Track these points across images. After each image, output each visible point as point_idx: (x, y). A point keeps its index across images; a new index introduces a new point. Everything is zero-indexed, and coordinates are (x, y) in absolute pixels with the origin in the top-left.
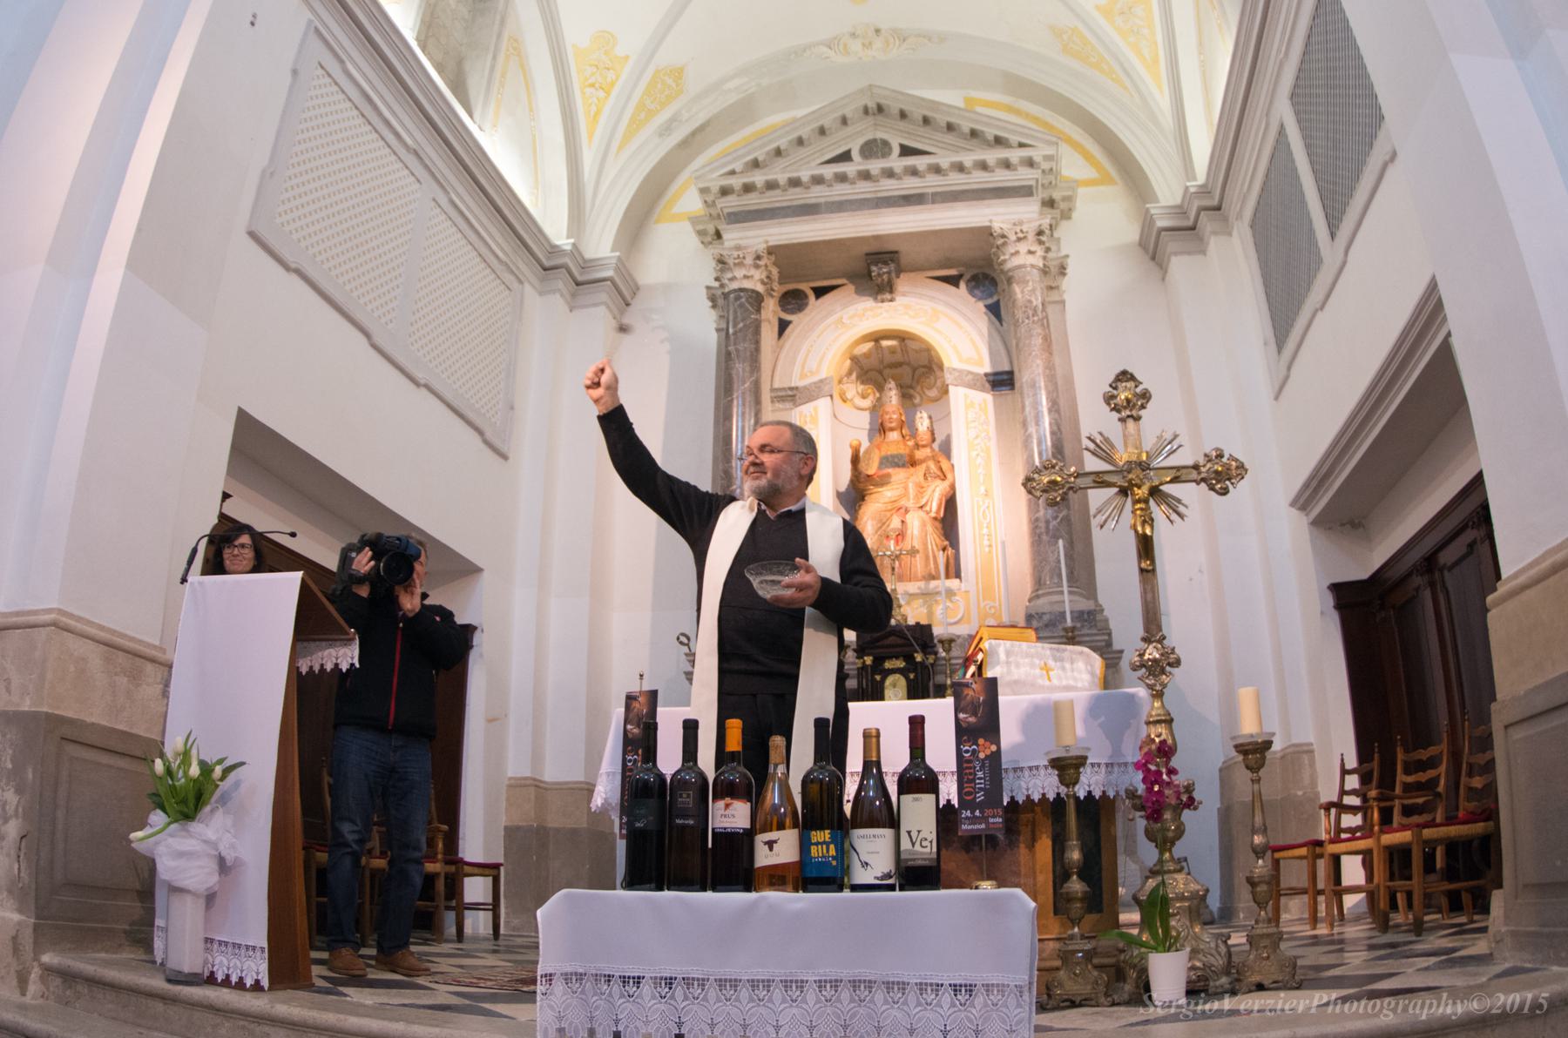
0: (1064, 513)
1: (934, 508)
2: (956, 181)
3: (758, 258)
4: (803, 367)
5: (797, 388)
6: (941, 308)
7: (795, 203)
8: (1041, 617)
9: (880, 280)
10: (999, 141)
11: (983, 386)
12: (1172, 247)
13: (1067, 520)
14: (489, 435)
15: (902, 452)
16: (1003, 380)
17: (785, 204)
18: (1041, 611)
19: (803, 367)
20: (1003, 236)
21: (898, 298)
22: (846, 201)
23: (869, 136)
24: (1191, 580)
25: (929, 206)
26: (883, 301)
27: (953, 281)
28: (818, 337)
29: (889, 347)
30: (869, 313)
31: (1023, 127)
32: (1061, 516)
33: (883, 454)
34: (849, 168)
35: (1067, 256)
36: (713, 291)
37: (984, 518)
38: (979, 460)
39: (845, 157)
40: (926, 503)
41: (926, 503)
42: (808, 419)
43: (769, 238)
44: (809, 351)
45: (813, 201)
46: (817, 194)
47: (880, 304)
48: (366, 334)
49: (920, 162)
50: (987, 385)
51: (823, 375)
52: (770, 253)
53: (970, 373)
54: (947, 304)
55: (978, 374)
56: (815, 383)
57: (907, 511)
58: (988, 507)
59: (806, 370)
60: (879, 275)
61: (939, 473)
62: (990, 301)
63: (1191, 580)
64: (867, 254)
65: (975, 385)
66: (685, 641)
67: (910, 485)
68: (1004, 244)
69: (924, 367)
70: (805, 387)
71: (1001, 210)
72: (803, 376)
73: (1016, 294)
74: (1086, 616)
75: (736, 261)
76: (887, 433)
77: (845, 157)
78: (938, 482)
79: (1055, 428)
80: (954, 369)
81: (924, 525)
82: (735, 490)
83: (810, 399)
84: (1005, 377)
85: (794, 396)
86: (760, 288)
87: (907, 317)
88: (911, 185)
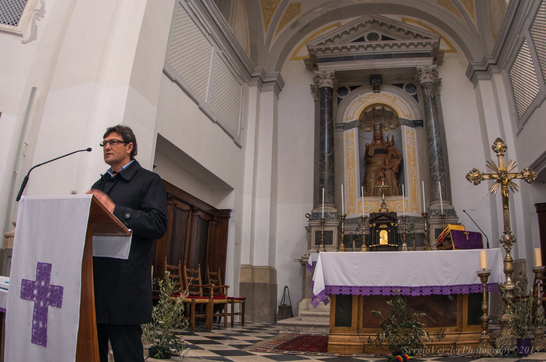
0: (443, 173)
1: (395, 170)
2: (404, 49)
3: (332, 75)
5: (345, 124)
6: (396, 96)
7: (344, 56)
9: (375, 85)
10: (417, 35)
11: (412, 125)
12: (479, 77)
13: (444, 176)
14: (236, 139)
15: (382, 148)
16: (419, 123)
17: (341, 56)
18: (435, 209)
19: (347, 116)
20: (420, 71)
21: (381, 92)
22: (363, 55)
23: (370, 32)
25: (394, 59)
26: (375, 92)
27: (400, 86)
28: (352, 105)
29: (378, 109)
30: (370, 97)
31: (427, 31)
32: (442, 174)
33: (375, 148)
34: (365, 44)
35: (441, 79)
36: (313, 87)
37: (413, 173)
38: (411, 153)
39: (362, 39)
40: (392, 167)
41: (392, 168)
42: (349, 135)
43: (335, 68)
44: (349, 111)
45: (351, 55)
46: (353, 53)
47: (375, 94)
48: (197, 103)
49: (390, 43)
50: (414, 125)
51: (355, 120)
52: (335, 74)
53: (408, 120)
54: (399, 95)
55: (411, 121)
56: (352, 122)
57: (385, 170)
58: (414, 170)
60: (375, 83)
61: (396, 156)
64: (370, 76)
65: (409, 125)
66: (309, 216)
67: (387, 160)
68: (421, 74)
69: (389, 117)
70: (348, 123)
71: (419, 61)
72: (347, 119)
73: (425, 93)
74: (451, 211)
75: (324, 77)
76: (376, 141)
77: (362, 39)
78: (396, 160)
80: (402, 119)
81: (391, 175)
82: (325, 161)
83: (350, 128)
84: (420, 122)
85: (344, 126)
86: (332, 86)
88: (387, 50)
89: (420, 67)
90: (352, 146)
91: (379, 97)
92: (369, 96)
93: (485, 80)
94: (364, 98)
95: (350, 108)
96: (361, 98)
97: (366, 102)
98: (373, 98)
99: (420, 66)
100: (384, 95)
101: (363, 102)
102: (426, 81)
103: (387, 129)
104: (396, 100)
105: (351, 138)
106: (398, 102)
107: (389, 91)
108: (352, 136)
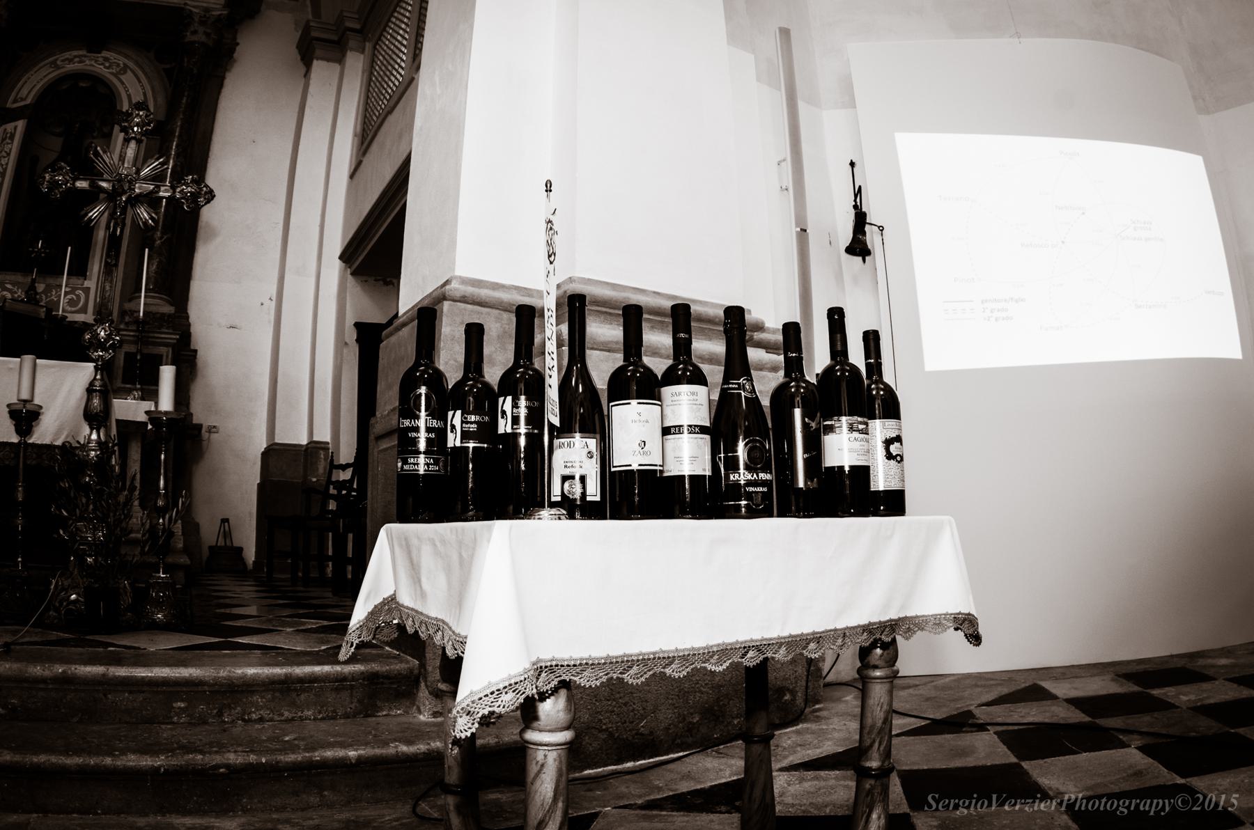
4: (17, 96)
8: (132, 314)
24: (262, 304)
28: (36, 72)
30: (77, 59)
32: (165, 237)
44: (26, 82)
59: (19, 96)
62: (168, 66)
63: (262, 304)
72: (15, 101)
74: (166, 318)
79: (179, 169)
87: (101, 67)
89: (190, 8)
90: (7, 159)
91: (93, 63)
92: (76, 57)
93: (328, 60)
94: (62, 61)
95: (29, 78)
96: (57, 60)
97: (63, 67)
98: (80, 62)
99: (194, 7)
100: (106, 59)
101: (58, 67)
102: (195, 38)
103: (95, 134)
104: (125, 72)
105: (10, 142)
106: (128, 78)
107: (119, 53)
108: (12, 137)
